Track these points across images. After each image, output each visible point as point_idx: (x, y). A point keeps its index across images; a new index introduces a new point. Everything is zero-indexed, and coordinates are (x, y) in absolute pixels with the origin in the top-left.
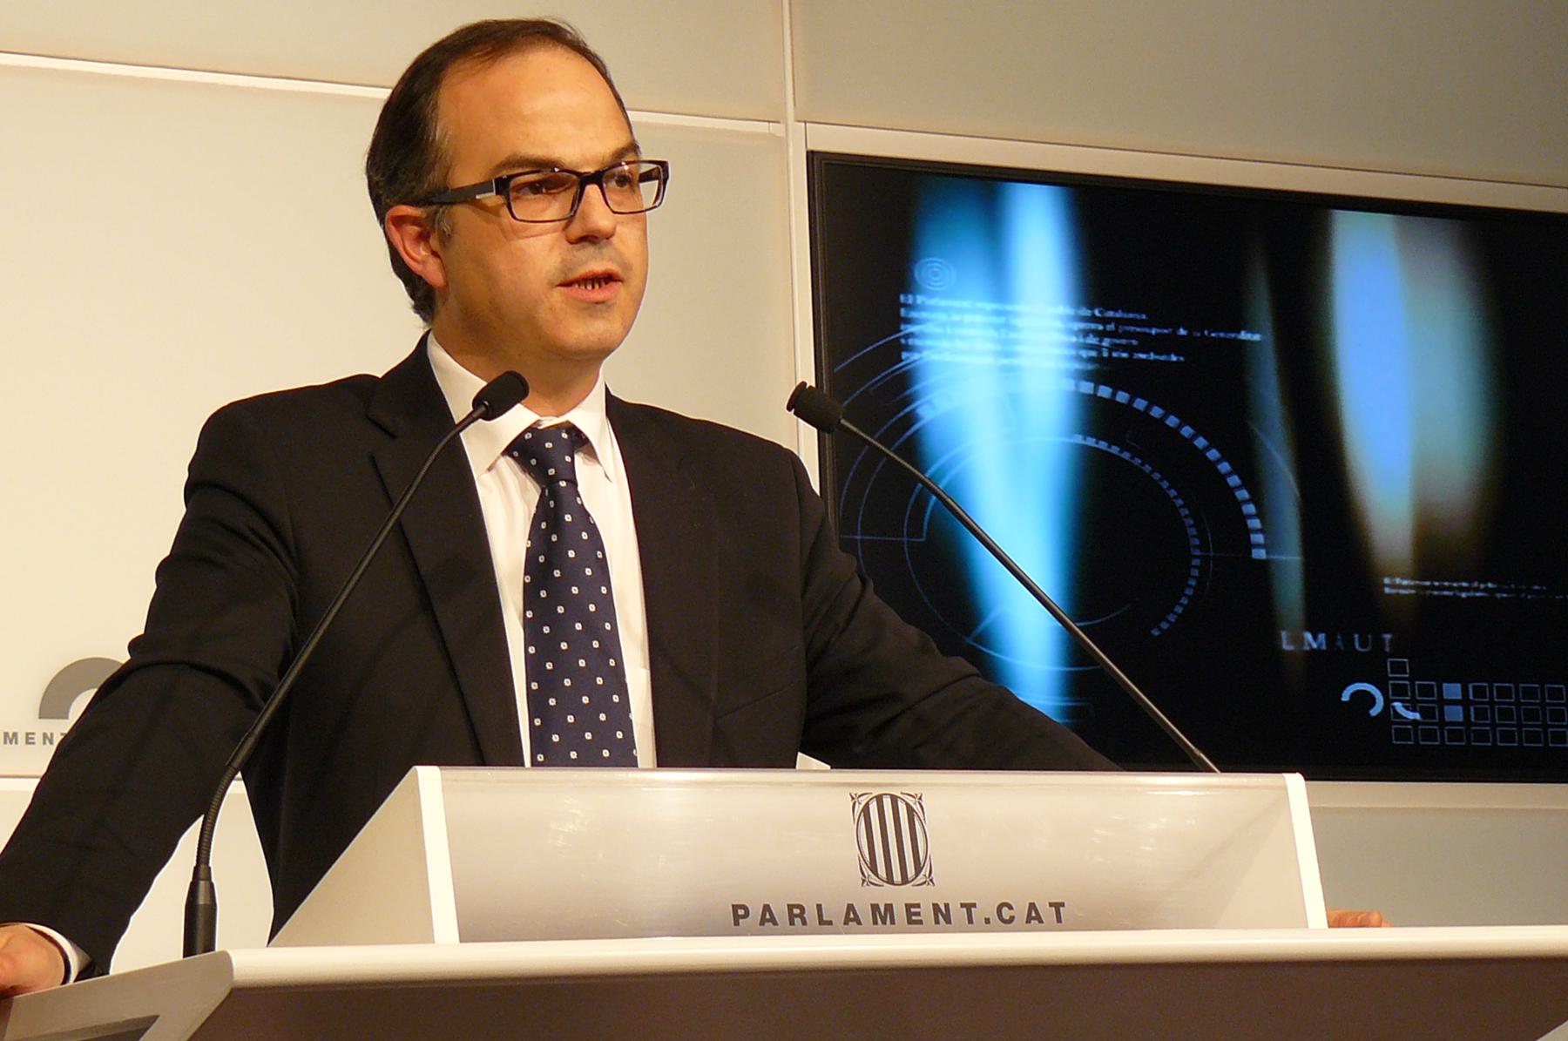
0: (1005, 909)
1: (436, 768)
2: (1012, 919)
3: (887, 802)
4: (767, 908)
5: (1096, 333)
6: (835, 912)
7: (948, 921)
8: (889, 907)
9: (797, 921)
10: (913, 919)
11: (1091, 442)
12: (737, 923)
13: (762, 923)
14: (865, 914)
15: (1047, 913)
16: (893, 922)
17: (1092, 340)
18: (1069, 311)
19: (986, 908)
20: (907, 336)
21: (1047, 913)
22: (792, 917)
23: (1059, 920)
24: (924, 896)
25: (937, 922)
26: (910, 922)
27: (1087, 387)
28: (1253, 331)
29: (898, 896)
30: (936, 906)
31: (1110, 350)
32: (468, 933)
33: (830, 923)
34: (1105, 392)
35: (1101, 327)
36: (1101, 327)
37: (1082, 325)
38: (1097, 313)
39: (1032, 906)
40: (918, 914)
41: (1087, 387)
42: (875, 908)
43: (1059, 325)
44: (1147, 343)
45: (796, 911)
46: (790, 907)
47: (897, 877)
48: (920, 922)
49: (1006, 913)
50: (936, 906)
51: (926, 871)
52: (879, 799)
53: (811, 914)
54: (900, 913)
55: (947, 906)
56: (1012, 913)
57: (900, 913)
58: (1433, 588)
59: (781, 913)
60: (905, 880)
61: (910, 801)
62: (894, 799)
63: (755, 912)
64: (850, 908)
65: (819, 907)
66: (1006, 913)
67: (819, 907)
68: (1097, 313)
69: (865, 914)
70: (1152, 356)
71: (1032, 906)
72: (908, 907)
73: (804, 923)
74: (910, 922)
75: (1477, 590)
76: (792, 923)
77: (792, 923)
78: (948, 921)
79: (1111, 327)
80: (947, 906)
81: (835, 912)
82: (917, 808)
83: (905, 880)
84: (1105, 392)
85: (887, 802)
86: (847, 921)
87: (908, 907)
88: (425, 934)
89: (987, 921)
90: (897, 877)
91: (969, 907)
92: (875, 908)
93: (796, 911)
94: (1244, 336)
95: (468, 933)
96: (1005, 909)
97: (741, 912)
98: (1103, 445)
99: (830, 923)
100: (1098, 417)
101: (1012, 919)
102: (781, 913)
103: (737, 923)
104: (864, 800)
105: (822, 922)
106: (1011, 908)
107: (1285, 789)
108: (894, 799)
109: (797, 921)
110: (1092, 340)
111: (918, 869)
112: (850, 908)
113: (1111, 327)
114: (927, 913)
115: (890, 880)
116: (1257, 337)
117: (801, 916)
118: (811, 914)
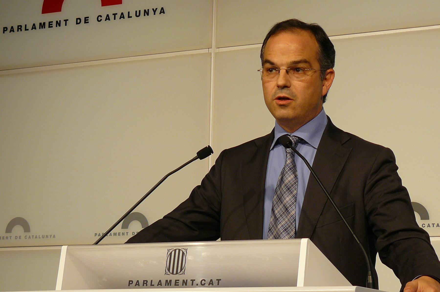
0: (203, 281)
2: (205, 284)
3: (177, 251)
4: (138, 281)
6: (155, 282)
7: (186, 284)
8: (171, 281)
9: (145, 285)
10: (176, 284)
12: (129, 285)
13: (135, 286)
14: (163, 282)
16: (170, 285)
19: (198, 281)
21: (215, 282)
22: (144, 283)
23: (218, 284)
24: (180, 277)
25: (183, 285)
26: (175, 285)
29: (173, 278)
30: (184, 280)
33: (154, 285)
39: (211, 280)
40: (178, 283)
42: (167, 281)
46: (144, 281)
47: (175, 272)
48: (178, 285)
50: (184, 280)
51: (183, 271)
52: (175, 250)
53: (149, 283)
54: (173, 283)
55: (187, 280)
57: (173, 283)
59: (141, 283)
60: (177, 273)
61: (184, 250)
62: (179, 250)
63: (135, 283)
64: (160, 281)
65: (152, 281)
67: (152, 281)
69: (163, 282)
71: (211, 280)
72: (176, 281)
73: (147, 285)
74: (175, 285)
76: (143, 285)
80: (187, 280)
81: (155, 282)
82: (185, 253)
83: (177, 273)
85: (177, 251)
87: (176, 281)
89: (197, 285)
90: (175, 272)
91: (193, 281)
92: (167, 281)
93: (145, 282)
96: (203, 281)
97: (131, 282)
99: (154, 285)
101: (205, 284)
102: (141, 283)
103: (129, 285)
104: (171, 251)
105: (151, 285)
106: (205, 280)
109: (145, 285)
112: (160, 281)
114: (181, 282)
115: (173, 273)
117: (146, 283)
118: (149, 283)
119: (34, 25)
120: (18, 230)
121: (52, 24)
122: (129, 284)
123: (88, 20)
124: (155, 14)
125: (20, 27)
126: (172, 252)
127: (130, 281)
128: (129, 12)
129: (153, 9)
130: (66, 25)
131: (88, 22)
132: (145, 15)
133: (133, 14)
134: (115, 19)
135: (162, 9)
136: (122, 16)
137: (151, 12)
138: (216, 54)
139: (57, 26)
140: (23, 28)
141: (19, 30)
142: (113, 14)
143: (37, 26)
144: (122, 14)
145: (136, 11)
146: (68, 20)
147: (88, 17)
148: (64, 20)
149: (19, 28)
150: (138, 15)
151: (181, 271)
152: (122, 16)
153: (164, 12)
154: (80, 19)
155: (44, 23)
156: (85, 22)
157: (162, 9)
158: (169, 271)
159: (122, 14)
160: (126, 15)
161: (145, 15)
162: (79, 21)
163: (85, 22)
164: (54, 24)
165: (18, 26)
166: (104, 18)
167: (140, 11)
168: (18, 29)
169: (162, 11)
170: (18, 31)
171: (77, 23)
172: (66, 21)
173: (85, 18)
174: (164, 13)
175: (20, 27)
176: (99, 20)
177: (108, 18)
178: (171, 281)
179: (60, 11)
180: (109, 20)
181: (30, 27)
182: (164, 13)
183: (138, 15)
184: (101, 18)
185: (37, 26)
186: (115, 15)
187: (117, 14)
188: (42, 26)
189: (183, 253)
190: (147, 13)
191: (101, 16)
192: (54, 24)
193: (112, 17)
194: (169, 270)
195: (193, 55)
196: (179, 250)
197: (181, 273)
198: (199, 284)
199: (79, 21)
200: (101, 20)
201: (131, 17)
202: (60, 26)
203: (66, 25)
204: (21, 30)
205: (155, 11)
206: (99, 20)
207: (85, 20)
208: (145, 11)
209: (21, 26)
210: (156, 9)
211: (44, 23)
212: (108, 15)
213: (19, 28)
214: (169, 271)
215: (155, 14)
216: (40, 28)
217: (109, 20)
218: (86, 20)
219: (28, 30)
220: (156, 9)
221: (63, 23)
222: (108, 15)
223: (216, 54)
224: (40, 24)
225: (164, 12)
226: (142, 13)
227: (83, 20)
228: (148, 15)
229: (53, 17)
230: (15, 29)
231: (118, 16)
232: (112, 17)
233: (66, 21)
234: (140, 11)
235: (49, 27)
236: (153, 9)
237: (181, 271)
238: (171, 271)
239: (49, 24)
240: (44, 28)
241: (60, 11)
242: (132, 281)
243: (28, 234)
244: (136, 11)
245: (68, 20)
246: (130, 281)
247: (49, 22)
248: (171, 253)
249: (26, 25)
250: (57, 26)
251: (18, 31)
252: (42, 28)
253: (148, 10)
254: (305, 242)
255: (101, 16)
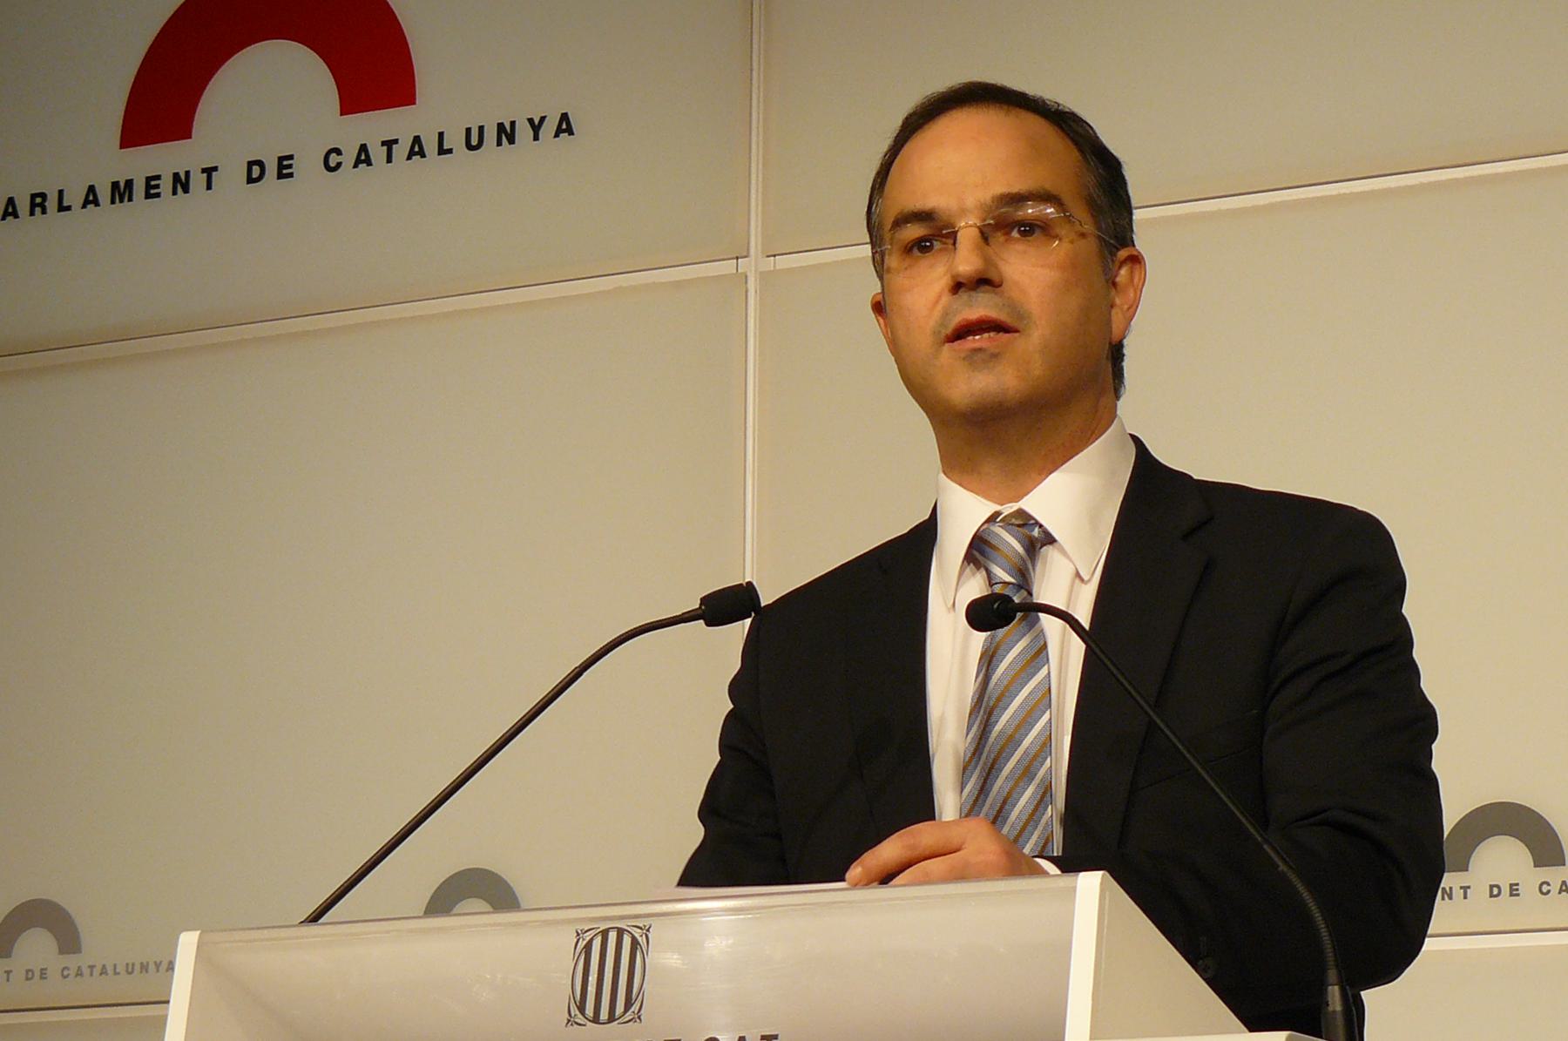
3: (613, 936)
47: (604, 1015)
51: (635, 1008)
60: (612, 1018)
61: (637, 933)
62: (620, 932)
82: (642, 940)
83: (612, 1018)
85: (613, 936)
90: (604, 1015)
104: (588, 936)
119: (91, 189)
120: (36, 946)
121: (157, 186)
123: (290, 166)
124: (536, 138)
125: (38, 200)
126: (590, 943)
128: (441, 135)
129: (531, 121)
130: (209, 187)
131: (291, 175)
132: (499, 143)
133: (455, 140)
134: (389, 160)
135: (565, 117)
136: (417, 149)
137: (524, 132)
138: (764, 277)
139: (175, 193)
140: (52, 204)
141: (38, 210)
142: (384, 143)
143: (104, 194)
144: (417, 140)
145: (468, 130)
146: (215, 169)
147: (291, 157)
148: (204, 171)
149: (38, 202)
150: (474, 142)
151: (626, 1011)
152: (417, 149)
153: (570, 131)
154: (260, 163)
155: (129, 183)
156: (280, 176)
157: (565, 117)
158: (583, 1013)
159: (417, 140)
160: (430, 146)
161: (499, 143)
162: (256, 171)
163: (280, 176)
164: (166, 185)
165: (33, 196)
166: (350, 155)
167: (481, 129)
168: (33, 205)
169: (565, 126)
170: (32, 214)
171: (250, 180)
172: (209, 171)
173: (281, 159)
174: (571, 133)
175: (38, 200)
176: (332, 164)
177: (363, 157)
179: (186, 134)
180: (369, 164)
181: (75, 197)
182: (571, 133)
183: (474, 142)
184: (339, 158)
185: (104, 194)
186: (389, 144)
187: (396, 141)
188: (121, 192)
189: (635, 943)
190: (506, 134)
191: (338, 151)
192: (166, 185)
193: (377, 153)
194: (582, 1009)
195: (678, 285)
196: (620, 932)
197: (628, 1016)
199: (256, 171)
200: (339, 165)
201: (450, 151)
202: (186, 191)
203: (209, 187)
204: (44, 212)
205: (536, 127)
206: (332, 164)
207: (281, 167)
208: (501, 126)
209: (43, 196)
210: (543, 119)
211: (129, 183)
212: (363, 148)
213: (38, 202)
214: (583, 1013)
215: (536, 138)
216: (113, 202)
217: (369, 164)
218: (284, 168)
219: (68, 208)
220: (543, 119)
221: (198, 180)
222: (363, 148)
223: (764, 277)
224: (115, 185)
225: (570, 131)
226: (491, 135)
227: (271, 169)
228: (511, 141)
229: (163, 158)
230: (23, 206)
231: (401, 151)
232: (377, 153)
233: (209, 171)
234: (481, 129)
235: (148, 196)
236: (531, 121)
237: (626, 1011)
238: (590, 1011)
239: (148, 187)
240: (130, 200)
241: (186, 134)
243: (72, 961)
244: (468, 130)
245: (215, 169)
247: (149, 179)
248: (588, 948)
249: (61, 192)
250: (175, 193)
251: (32, 214)
252: (121, 201)
253: (513, 124)
254: (1091, 883)
255: (338, 151)
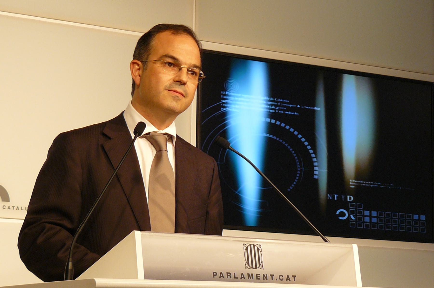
1: (139, 231)
2: (283, 279)
3: (252, 246)
4: (221, 273)
5: (275, 105)
6: (238, 275)
7: (267, 279)
8: (252, 275)
9: (229, 277)
11: (268, 135)
12: (214, 277)
14: (246, 276)
15: (292, 278)
17: (273, 107)
18: (268, 99)
19: (276, 276)
20: (224, 103)
21: (292, 278)
22: (228, 276)
26: (257, 279)
27: (268, 120)
28: (317, 107)
29: (254, 272)
30: (264, 275)
31: (279, 110)
32: (147, 277)
33: (237, 278)
34: (273, 121)
35: (276, 104)
36: (276, 104)
37: (271, 103)
38: (275, 99)
39: (288, 276)
41: (268, 120)
42: (248, 274)
43: (265, 102)
44: (289, 109)
45: (229, 274)
46: (227, 273)
48: (260, 279)
49: (281, 278)
50: (264, 275)
51: (261, 265)
52: (250, 245)
55: (266, 275)
56: (283, 278)
58: (363, 183)
59: (225, 275)
60: (256, 268)
61: (258, 246)
62: (254, 246)
63: (219, 274)
64: (242, 274)
65: (234, 274)
66: (281, 278)
67: (234, 274)
68: (275, 99)
69: (246, 276)
70: (290, 113)
71: (288, 276)
73: (231, 278)
74: (257, 279)
75: (375, 184)
76: (228, 278)
77: (228, 278)
78: (267, 279)
79: (279, 104)
80: (266, 275)
81: (238, 275)
82: (260, 248)
84: (273, 121)
85: (252, 246)
86: (241, 278)
87: (257, 275)
88: (136, 277)
89: (276, 280)
91: (272, 276)
92: (248, 274)
93: (229, 274)
94: (315, 108)
95: (147, 277)
97: (215, 274)
98: (271, 136)
100: (271, 129)
101: (283, 279)
102: (225, 275)
103: (214, 277)
104: (246, 246)
105: (235, 278)
107: (352, 248)
108: (254, 246)
109: (229, 277)
110: (273, 107)
111: (260, 265)
112: (242, 274)
113: (279, 104)
115: (252, 267)
116: (319, 109)
117: (230, 276)
118: (232, 275)
122: (214, 276)
126: (247, 247)
127: (214, 273)
178: (252, 275)
189: (258, 249)
194: (248, 264)
197: (260, 267)
198: (278, 279)
237: (259, 266)
242: (215, 273)
246: (214, 273)
248: (247, 248)
